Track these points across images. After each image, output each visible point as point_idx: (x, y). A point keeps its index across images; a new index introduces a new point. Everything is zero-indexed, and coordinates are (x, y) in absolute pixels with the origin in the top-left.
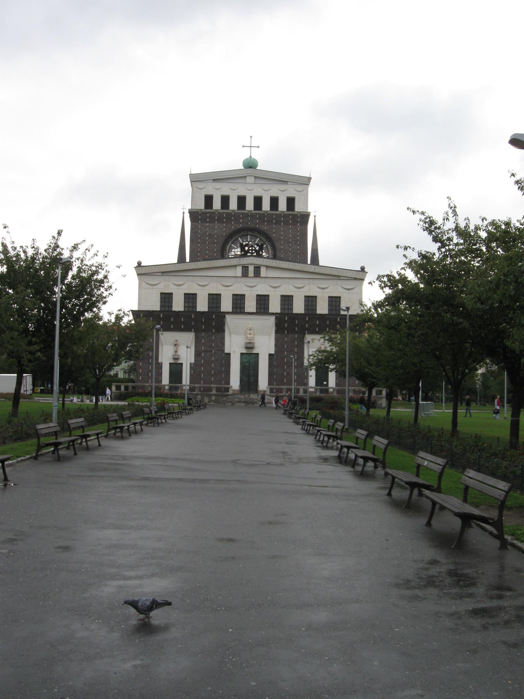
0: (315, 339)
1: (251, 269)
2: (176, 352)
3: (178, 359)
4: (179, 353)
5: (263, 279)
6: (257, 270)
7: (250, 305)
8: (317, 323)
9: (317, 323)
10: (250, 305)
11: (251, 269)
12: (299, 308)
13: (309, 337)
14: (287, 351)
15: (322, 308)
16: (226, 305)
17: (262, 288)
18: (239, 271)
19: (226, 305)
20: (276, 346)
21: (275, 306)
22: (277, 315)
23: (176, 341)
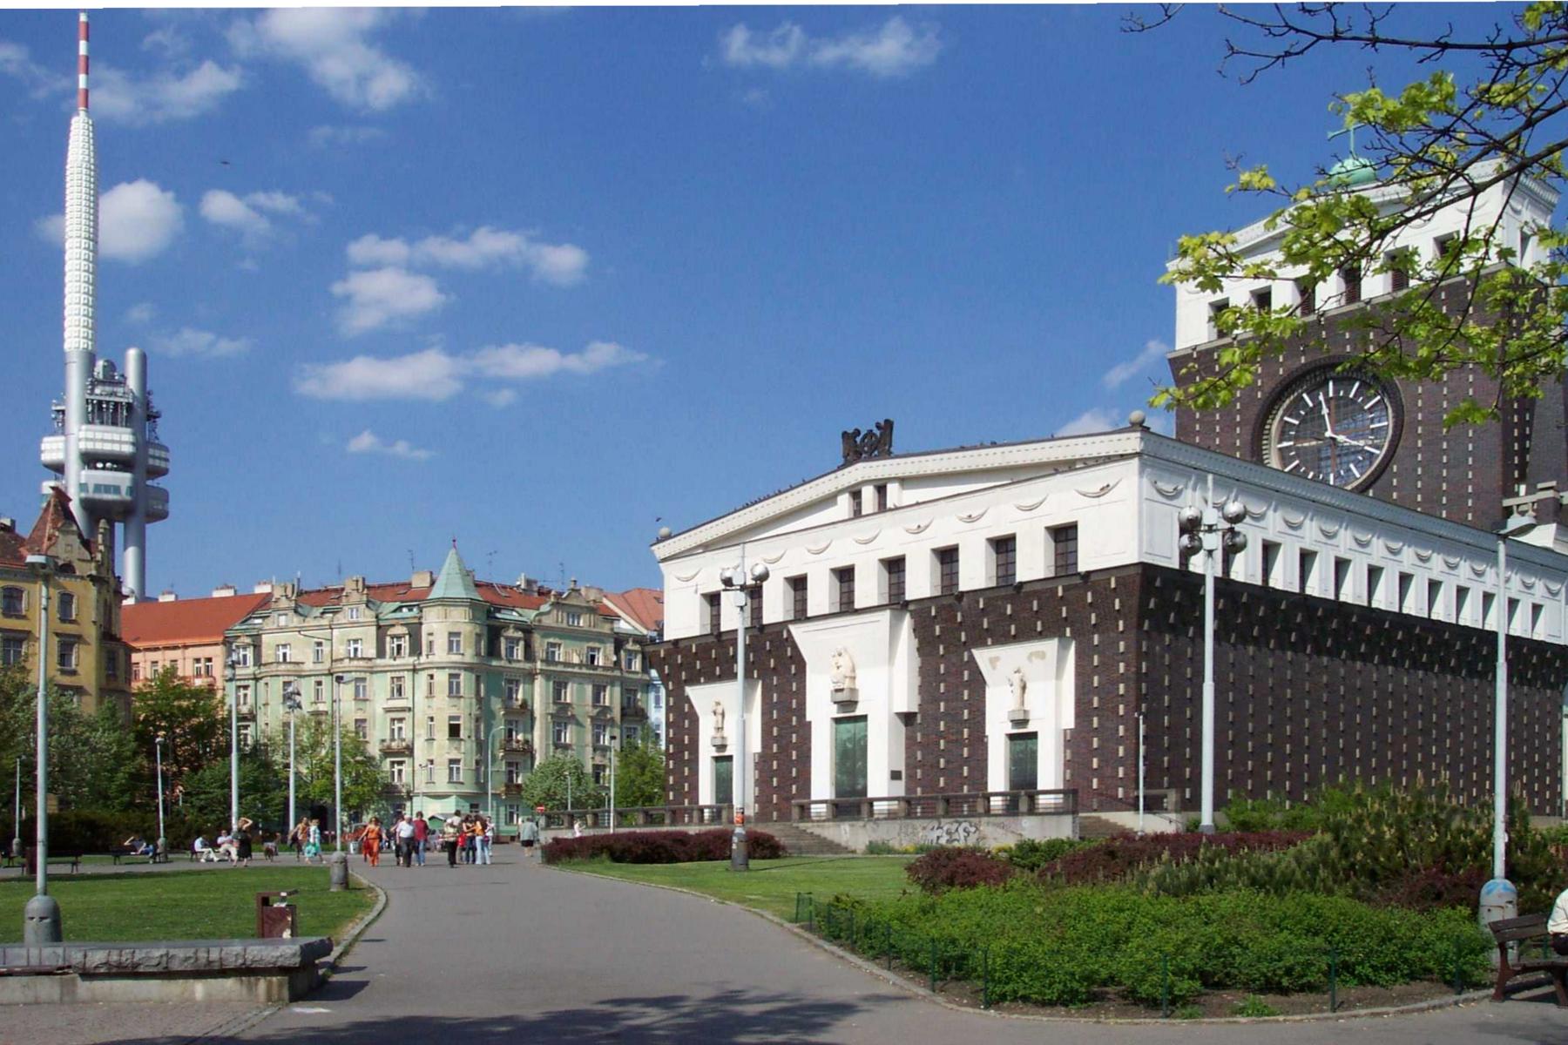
0: (997, 659)
1: (868, 494)
2: (720, 729)
3: (722, 747)
4: (726, 733)
5: (888, 514)
6: (881, 489)
7: (869, 588)
8: (1009, 612)
9: (1009, 612)
10: (869, 588)
11: (868, 494)
12: (975, 573)
13: (982, 656)
14: (947, 701)
15: (1033, 563)
16: (821, 596)
17: (891, 536)
18: (845, 501)
19: (821, 596)
20: (922, 689)
21: (921, 583)
22: (911, 607)
23: (718, 704)
